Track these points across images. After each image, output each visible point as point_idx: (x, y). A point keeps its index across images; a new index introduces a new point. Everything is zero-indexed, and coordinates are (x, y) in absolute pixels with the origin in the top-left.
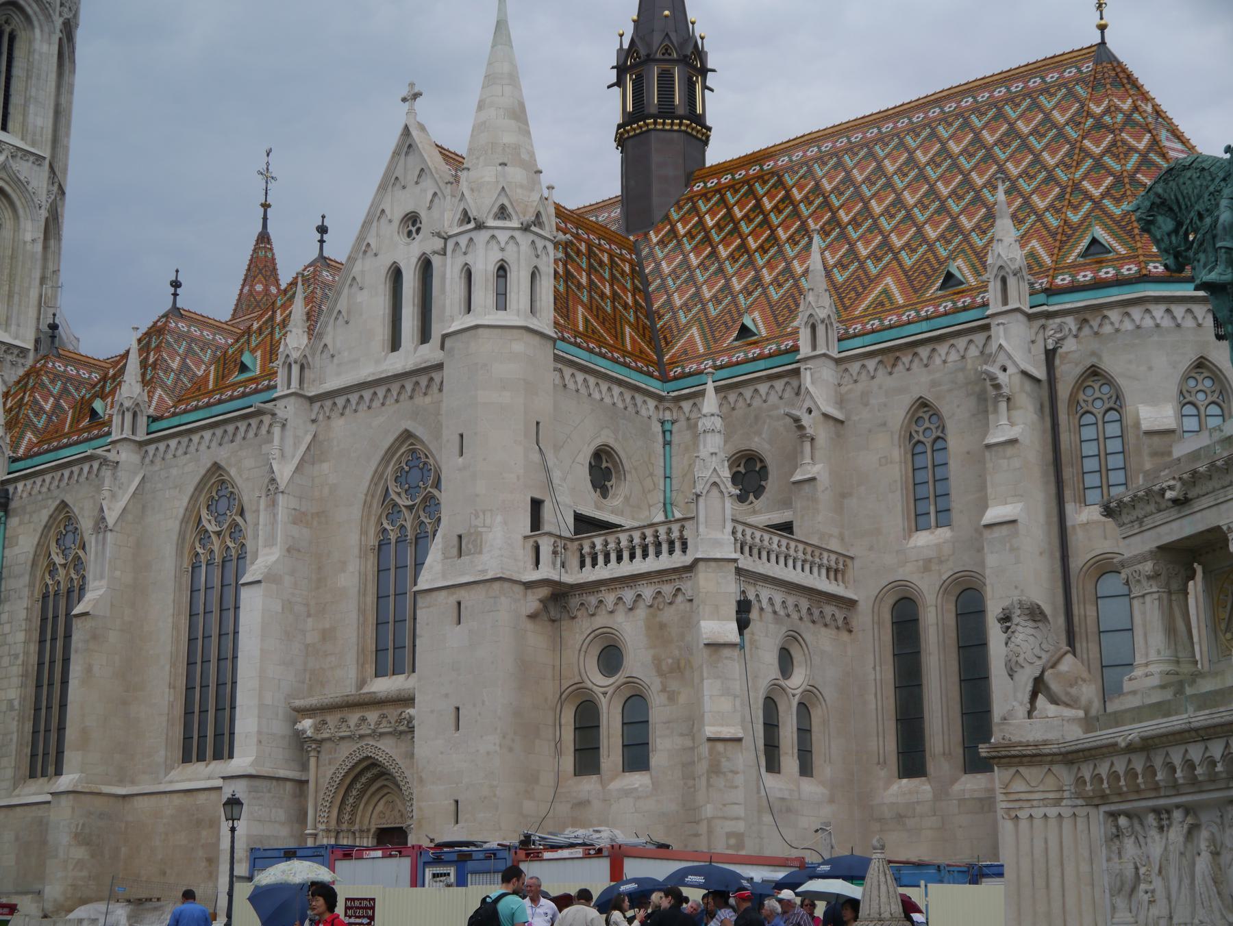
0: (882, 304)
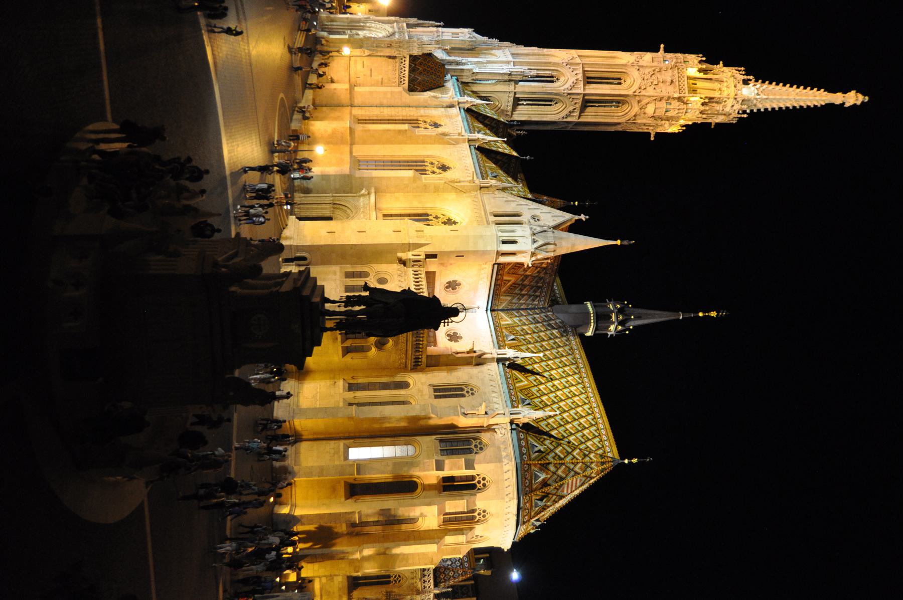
0: (516, 379)
